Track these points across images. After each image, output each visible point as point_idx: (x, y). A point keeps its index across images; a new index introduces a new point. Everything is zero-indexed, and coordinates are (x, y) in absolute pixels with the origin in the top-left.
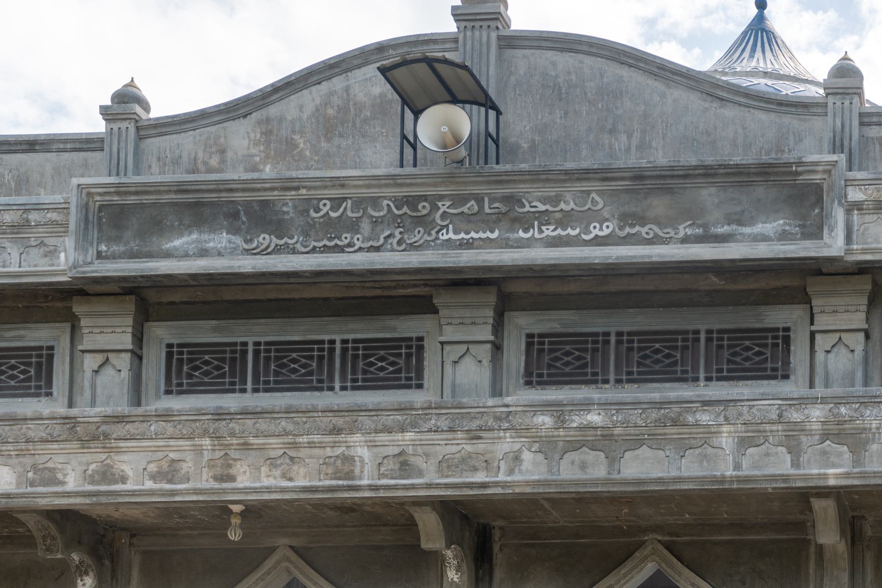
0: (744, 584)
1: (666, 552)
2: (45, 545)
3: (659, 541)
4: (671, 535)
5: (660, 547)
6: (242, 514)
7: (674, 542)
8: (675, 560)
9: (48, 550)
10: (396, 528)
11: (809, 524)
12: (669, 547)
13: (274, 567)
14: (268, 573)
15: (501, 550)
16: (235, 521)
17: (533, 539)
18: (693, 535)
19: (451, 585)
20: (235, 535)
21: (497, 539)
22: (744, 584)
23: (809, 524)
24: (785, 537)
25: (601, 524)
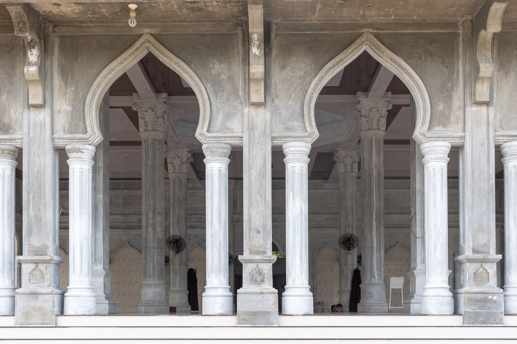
0: (421, 59)
1: (375, 39)
2: (19, 28)
3: (371, 33)
4: (378, 29)
5: (372, 37)
6: (136, 10)
7: (379, 34)
8: (381, 44)
9: (21, 30)
10: (214, 23)
11: (459, 24)
12: (376, 36)
13: (141, 46)
14: (137, 50)
15: (276, 37)
16: (133, 14)
17: (295, 31)
18: (391, 30)
19: (255, 57)
20: (132, 24)
21: (274, 30)
22: (421, 59)
23: (459, 24)
24: (445, 31)
25: (337, 22)
